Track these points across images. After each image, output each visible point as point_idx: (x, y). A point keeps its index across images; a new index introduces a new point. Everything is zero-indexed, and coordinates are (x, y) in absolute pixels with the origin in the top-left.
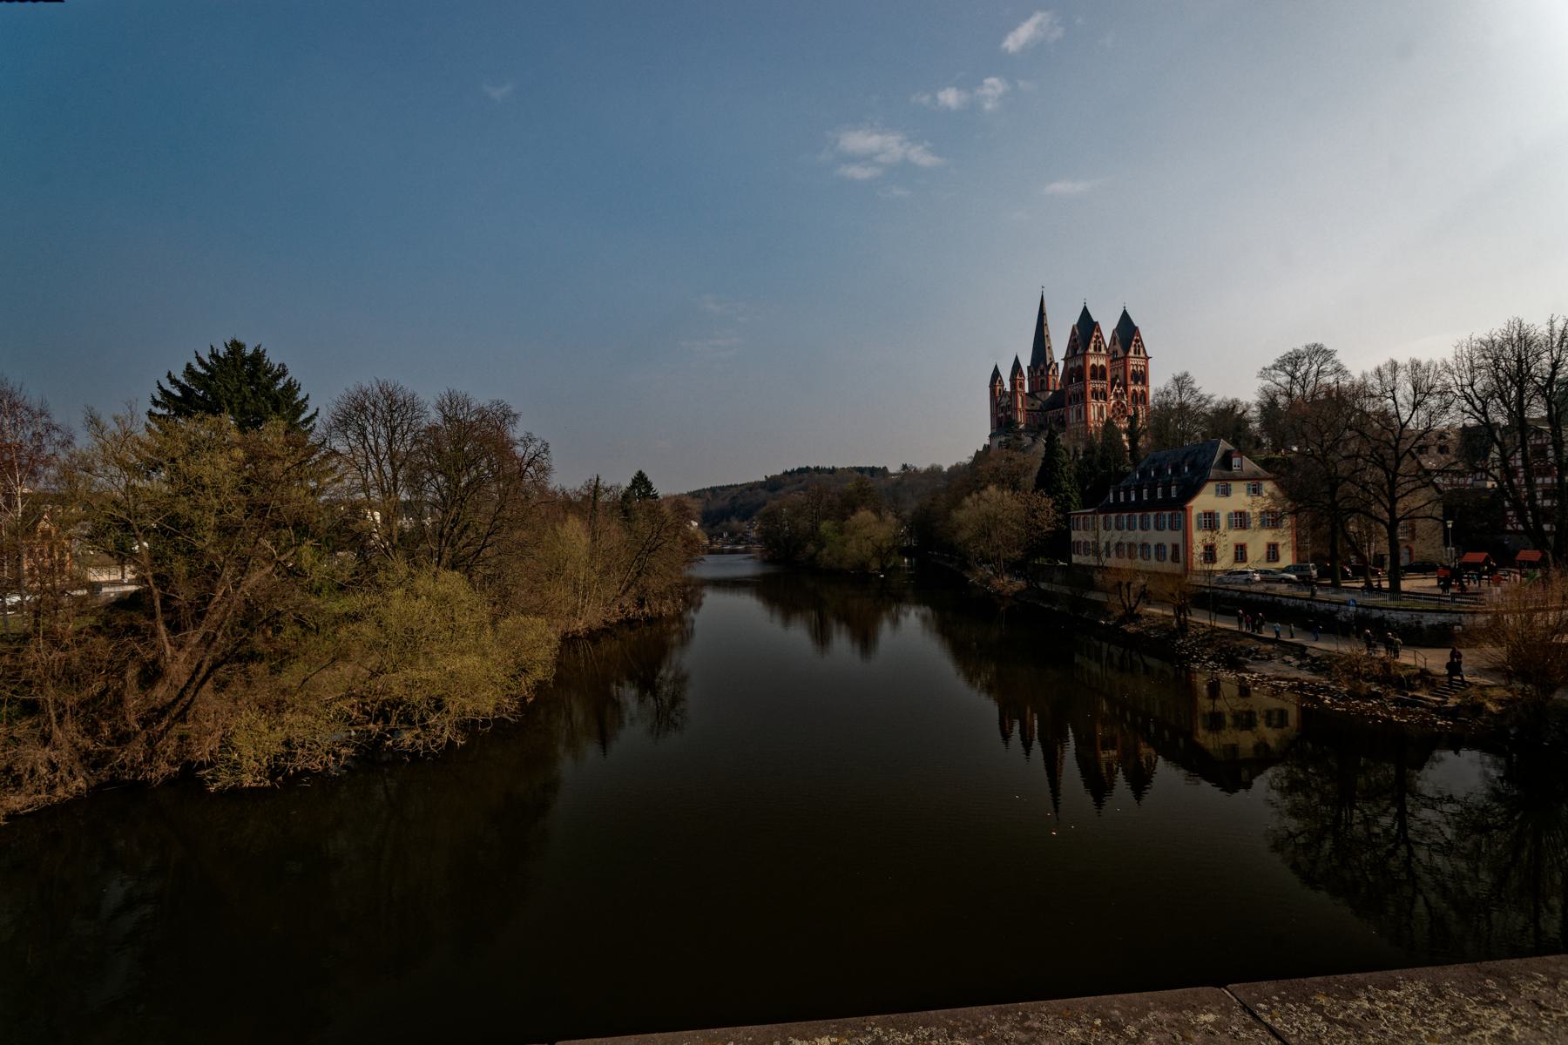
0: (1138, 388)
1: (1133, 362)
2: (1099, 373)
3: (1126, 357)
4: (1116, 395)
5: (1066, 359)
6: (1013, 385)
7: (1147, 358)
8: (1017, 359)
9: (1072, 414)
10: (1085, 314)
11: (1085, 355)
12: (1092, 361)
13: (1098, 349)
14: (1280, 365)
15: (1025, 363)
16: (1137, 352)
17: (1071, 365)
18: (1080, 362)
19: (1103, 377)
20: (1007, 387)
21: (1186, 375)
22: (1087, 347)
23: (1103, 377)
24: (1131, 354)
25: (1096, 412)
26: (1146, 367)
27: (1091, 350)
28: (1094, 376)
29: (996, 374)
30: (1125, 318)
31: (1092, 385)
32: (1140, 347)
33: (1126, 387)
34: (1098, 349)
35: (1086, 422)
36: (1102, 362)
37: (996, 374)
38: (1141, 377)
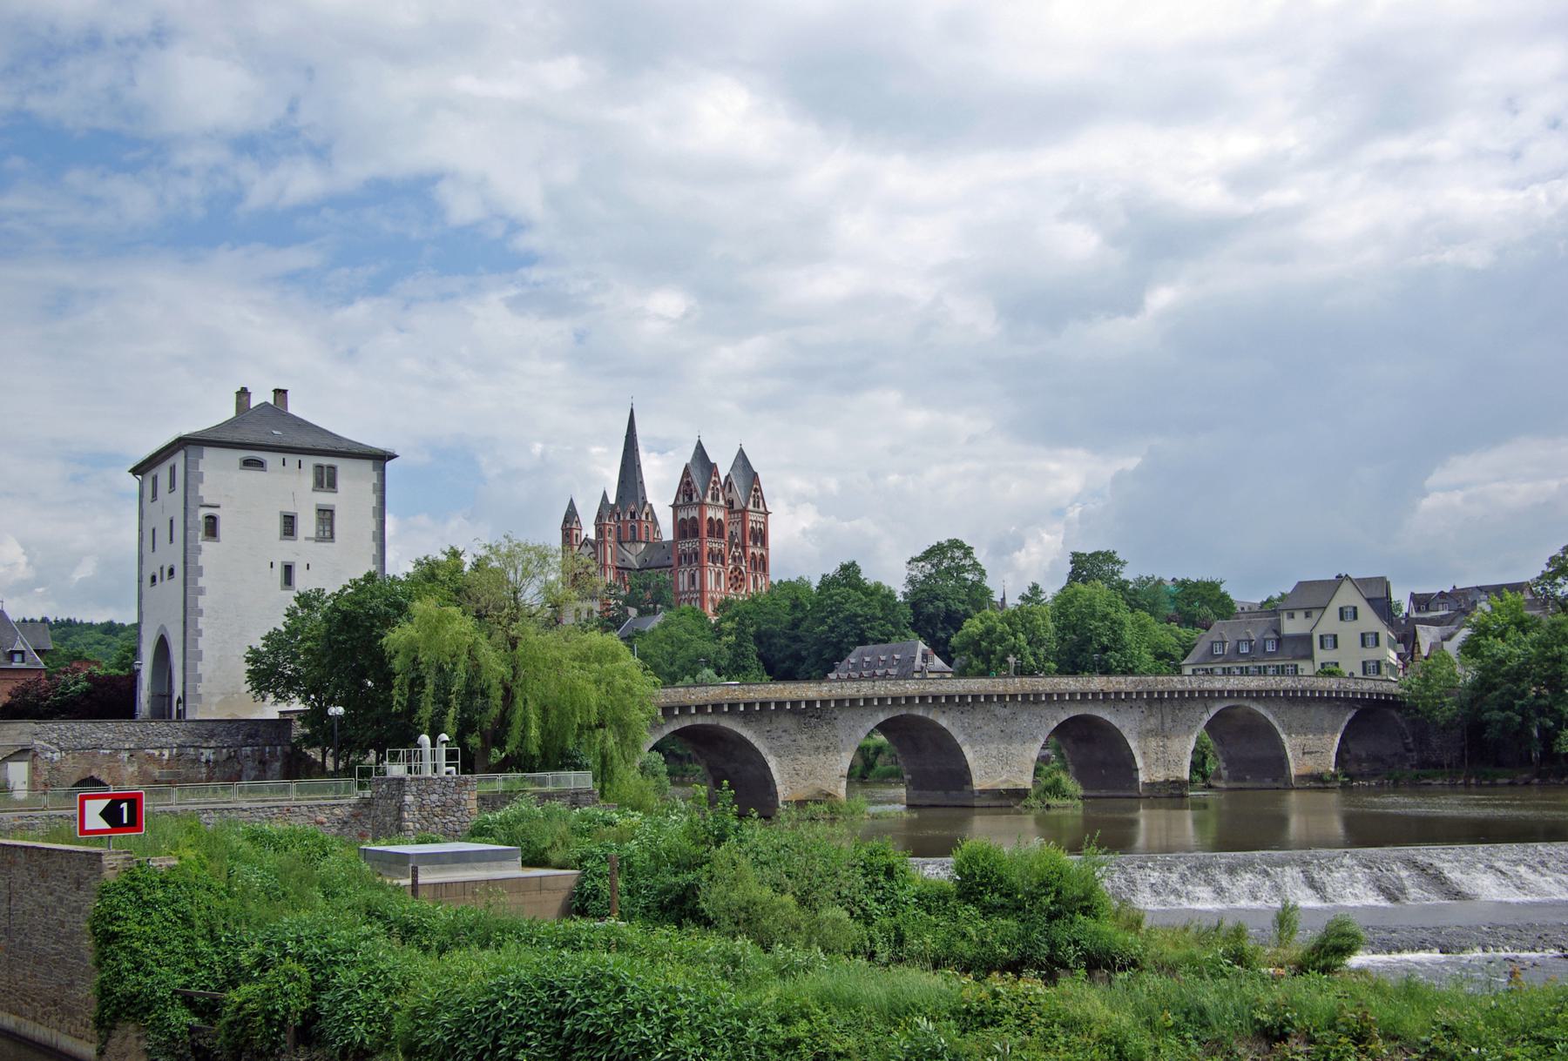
0: (758, 552)
1: (752, 517)
2: (716, 529)
3: (744, 511)
4: (734, 558)
5: (675, 507)
6: (600, 531)
7: (767, 513)
8: (605, 497)
9: (683, 580)
10: (700, 452)
11: (701, 504)
12: (710, 513)
13: (715, 497)
14: (928, 555)
15: (612, 500)
16: (756, 504)
17: (682, 515)
18: (694, 513)
19: (721, 535)
20: (589, 532)
21: (853, 564)
22: (705, 495)
23: (721, 535)
24: (750, 507)
25: (715, 584)
26: (765, 524)
27: (709, 500)
28: (711, 533)
29: (571, 515)
30: (742, 459)
31: (711, 544)
32: (759, 500)
33: (744, 548)
34: (715, 497)
35: (702, 591)
36: (720, 515)
37: (571, 515)
38: (761, 537)
